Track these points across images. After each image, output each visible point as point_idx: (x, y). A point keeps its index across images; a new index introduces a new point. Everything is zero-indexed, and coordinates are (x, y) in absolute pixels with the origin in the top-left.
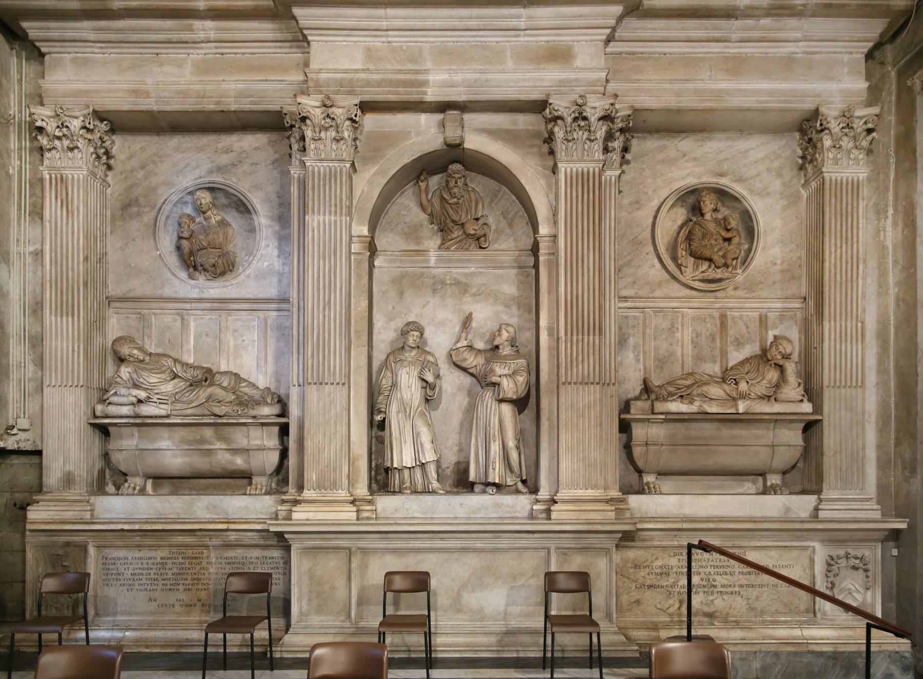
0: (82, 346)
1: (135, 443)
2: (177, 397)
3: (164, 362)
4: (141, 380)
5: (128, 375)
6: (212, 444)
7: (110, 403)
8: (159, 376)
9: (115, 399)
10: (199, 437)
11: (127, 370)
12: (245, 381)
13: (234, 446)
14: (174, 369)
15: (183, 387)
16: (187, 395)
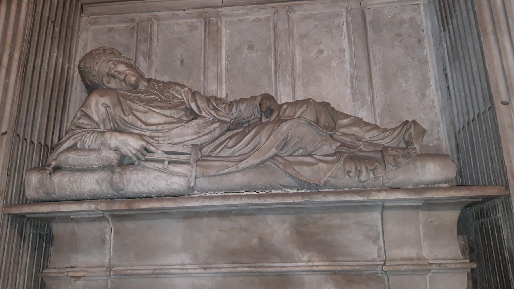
0: (16, 56)
1: (106, 261)
2: (206, 150)
3: (174, 93)
4: (130, 119)
5: (102, 109)
6: (289, 258)
7: (57, 169)
8: (167, 112)
9: (72, 158)
10: (255, 241)
11: (102, 100)
12: (347, 116)
13: (347, 265)
14: (193, 105)
15: (216, 133)
16: (231, 143)
